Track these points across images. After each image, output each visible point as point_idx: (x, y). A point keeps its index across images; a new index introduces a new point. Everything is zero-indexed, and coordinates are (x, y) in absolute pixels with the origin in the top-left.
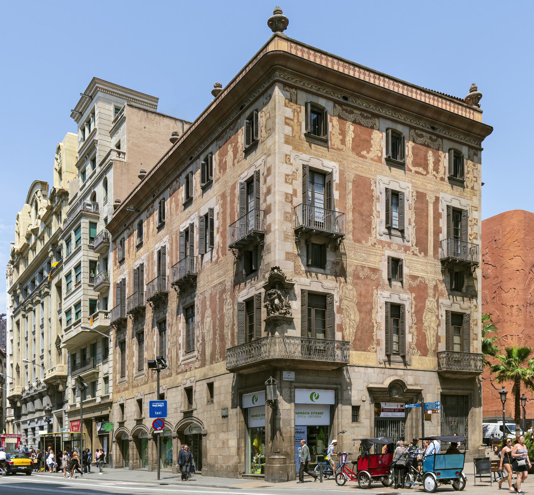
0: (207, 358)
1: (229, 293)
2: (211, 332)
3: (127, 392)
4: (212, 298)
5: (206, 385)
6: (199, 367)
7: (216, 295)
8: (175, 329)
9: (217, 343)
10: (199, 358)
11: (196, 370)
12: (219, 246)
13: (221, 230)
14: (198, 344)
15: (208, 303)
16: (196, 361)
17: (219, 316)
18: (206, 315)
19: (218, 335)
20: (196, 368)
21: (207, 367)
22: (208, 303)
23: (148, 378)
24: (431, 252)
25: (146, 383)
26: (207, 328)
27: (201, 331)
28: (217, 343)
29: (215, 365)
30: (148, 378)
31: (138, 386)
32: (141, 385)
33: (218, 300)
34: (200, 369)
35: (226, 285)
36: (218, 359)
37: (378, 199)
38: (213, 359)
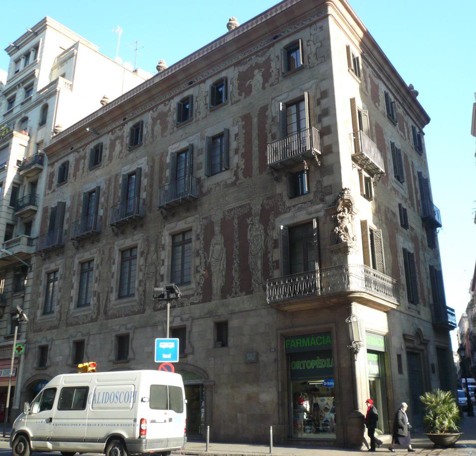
0: (215, 292)
1: (258, 218)
2: (224, 263)
3: (55, 331)
4: (225, 224)
5: (212, 324)
6: (199, 303)
7: (233, 219)
8: (154, 257)
9: (235, 275)
10: (200, 290)
11: (193, 306)
12: (238, 167)
13: (242, 150)
14: (198, 276)
15: (217, 229)
16: (193, 295)
17: (238, 243)
18: (214, 241)
19: (236, 265)
20: (192, 304)
21: (213, 303)
22: (217, 229)
23: (98, 313)
24: (416, 209)
25: (92, 320)
26: (216, 256)
27: (203, 261)
28: (235, 275)
29: (230, 300)
30: (98, 313)
31: (78, 324)
32: (83, 323)
33: (236, 226)
34: (201, 304)
35: (251, 209)
36: (236, 293)
37: (388, 148)
38: (226, 292)
